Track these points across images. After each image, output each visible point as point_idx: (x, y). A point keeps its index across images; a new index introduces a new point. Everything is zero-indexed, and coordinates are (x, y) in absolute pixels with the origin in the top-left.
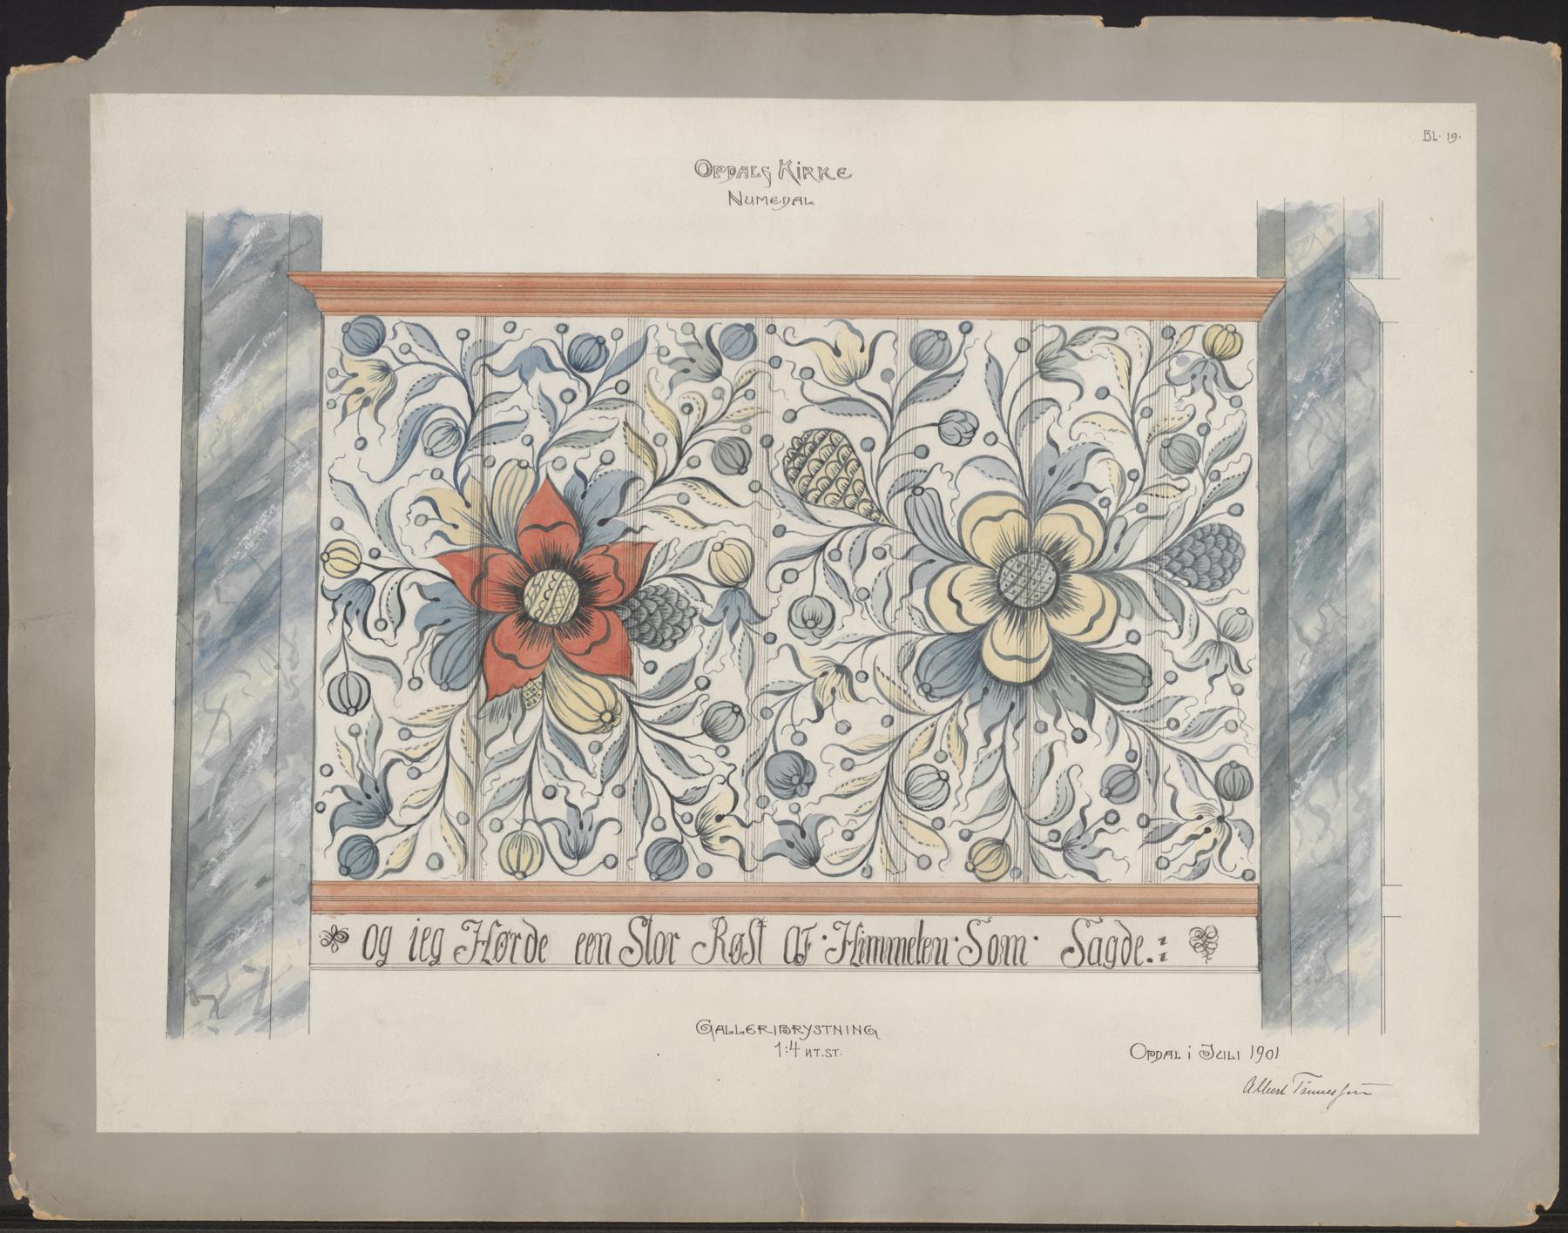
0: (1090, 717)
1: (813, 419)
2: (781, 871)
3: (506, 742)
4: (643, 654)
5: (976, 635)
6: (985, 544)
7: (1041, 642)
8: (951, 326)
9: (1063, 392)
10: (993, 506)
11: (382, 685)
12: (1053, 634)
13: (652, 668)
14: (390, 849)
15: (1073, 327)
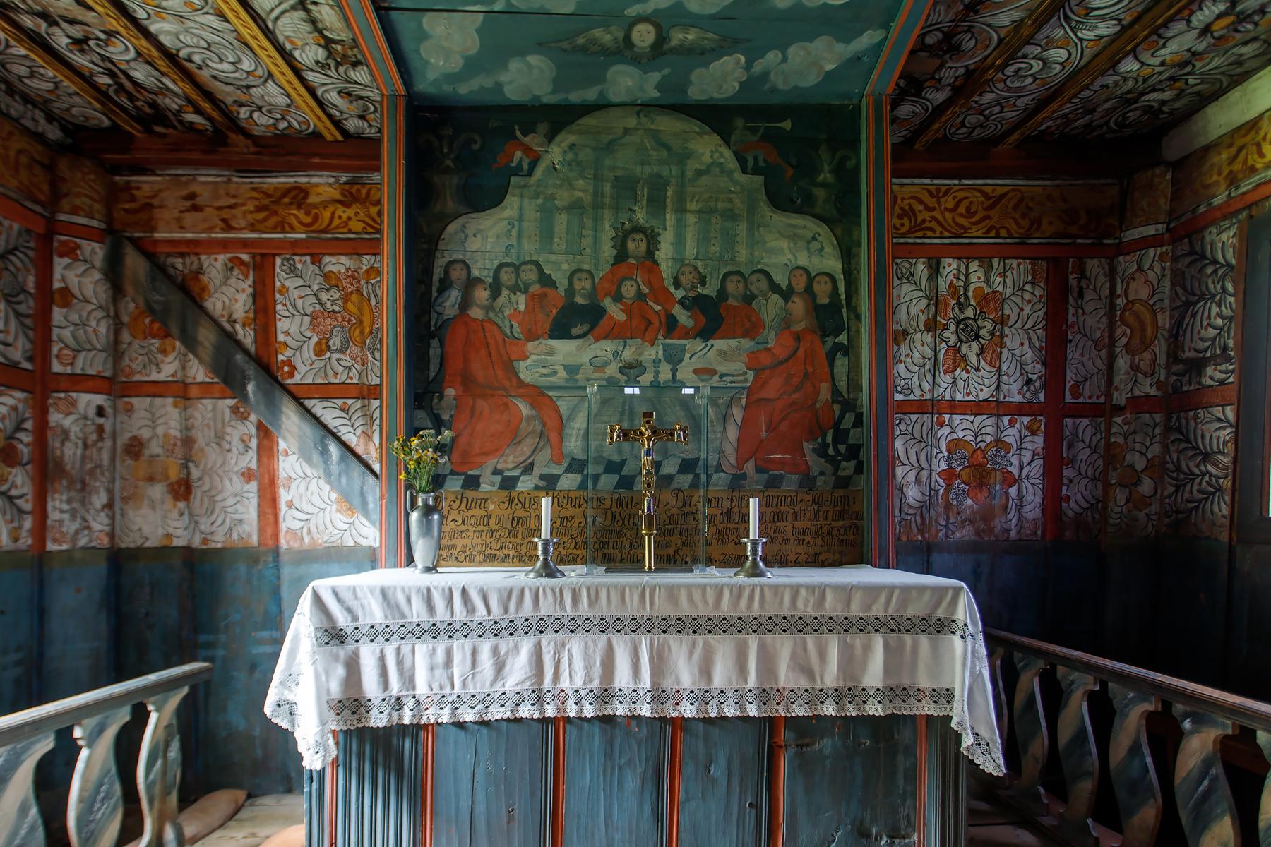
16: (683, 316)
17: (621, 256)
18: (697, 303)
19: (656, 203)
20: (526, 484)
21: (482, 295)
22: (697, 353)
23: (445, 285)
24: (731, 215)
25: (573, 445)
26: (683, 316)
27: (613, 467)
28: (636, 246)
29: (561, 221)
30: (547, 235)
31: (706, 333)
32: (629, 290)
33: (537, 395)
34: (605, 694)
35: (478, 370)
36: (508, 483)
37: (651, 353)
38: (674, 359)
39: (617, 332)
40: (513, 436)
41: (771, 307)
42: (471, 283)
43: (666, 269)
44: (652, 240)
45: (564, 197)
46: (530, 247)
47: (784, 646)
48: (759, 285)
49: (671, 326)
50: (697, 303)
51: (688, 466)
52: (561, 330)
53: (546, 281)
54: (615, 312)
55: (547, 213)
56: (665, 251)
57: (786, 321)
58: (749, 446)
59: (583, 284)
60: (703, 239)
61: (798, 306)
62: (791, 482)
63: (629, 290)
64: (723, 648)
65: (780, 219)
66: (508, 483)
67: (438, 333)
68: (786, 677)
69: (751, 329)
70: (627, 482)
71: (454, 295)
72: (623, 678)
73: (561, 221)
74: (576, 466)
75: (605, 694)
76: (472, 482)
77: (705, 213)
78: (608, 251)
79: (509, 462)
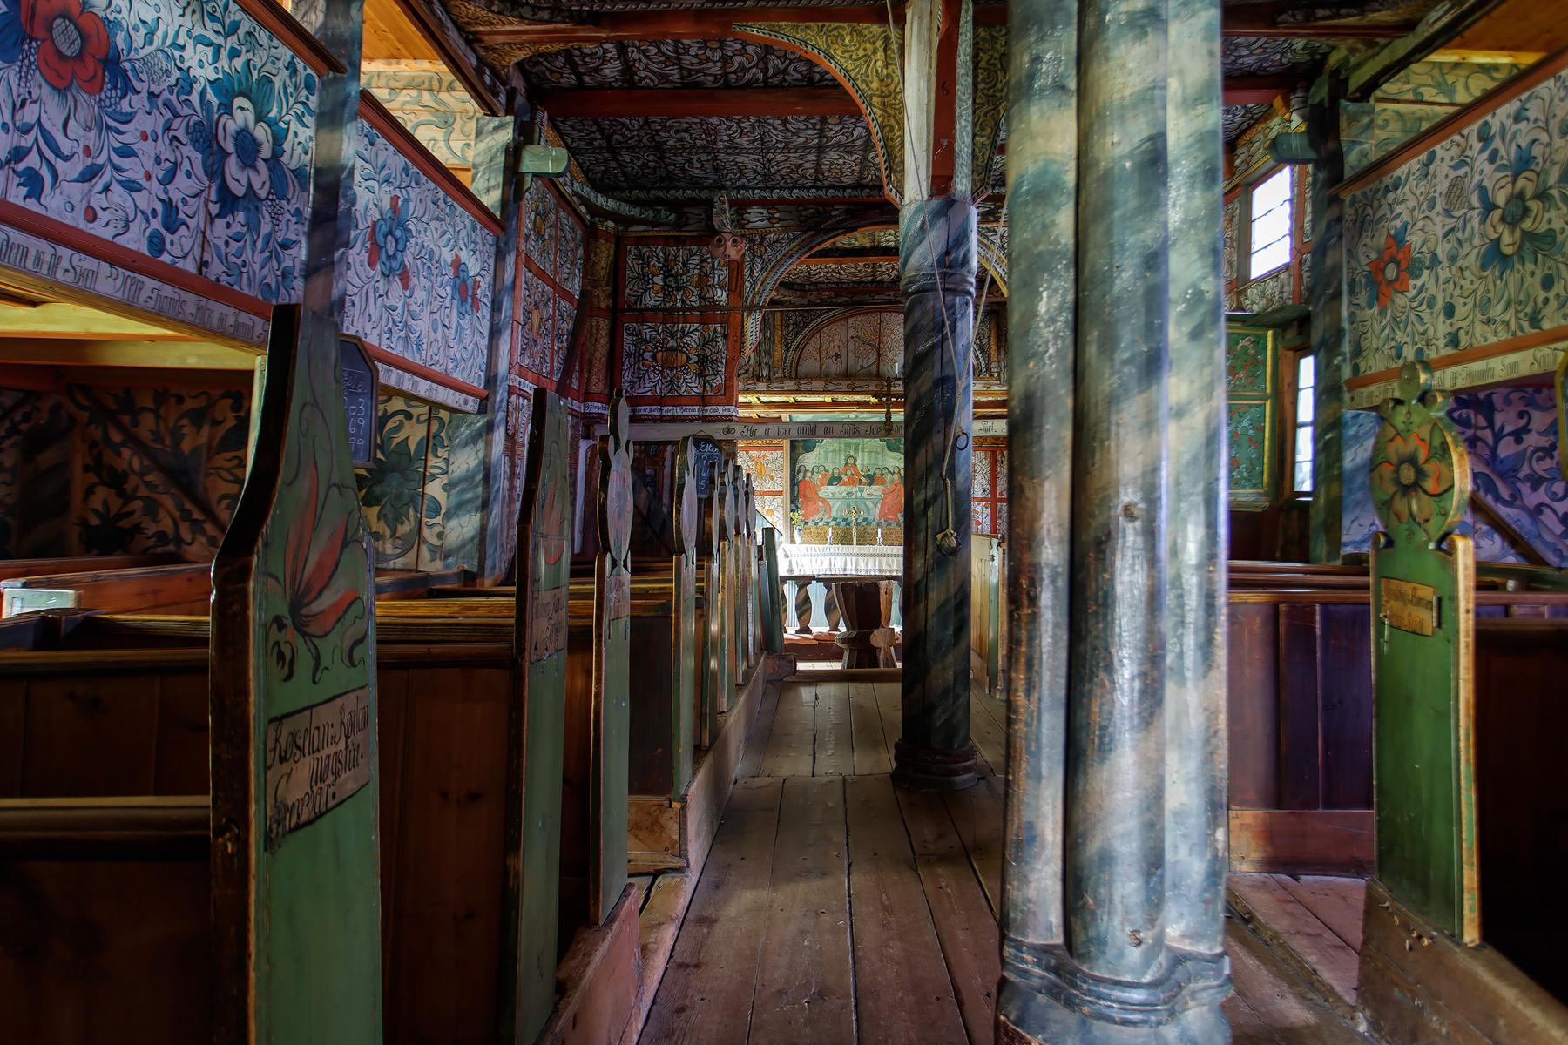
0: (1536, 262)
1: (1453, 174)
2: (1450, 351)
3: (1384, 322)
4: (1412, 282)
5: (1498, 240)
6: (1501, 199)
7: (1518, 233)
8: (1488, 118)
9: (1523, 125)
10: (1503, 182)
11: (1358, 312)
12: (1523, 231)
13: (1415, 287)
14: (1362, 366)
15: (1524, 97)
16: (864, 480)
17: (847, 464)
18: (868, 476)
19: (856, 450)
20: (821, 524)
21: (809, 474)
22: (868, 490)
23: (799, 471)
24: (877, 453)
25: (834, 514)
26: (864, 480)
27: (844, 520)
28: (851, 461)
29: (830, 455)
30: (826, 459)
31: (870, 484)
32: (849, 473)
33: (824, 500)
34: (845, 569)
35: (808, 494)
36: (816, 524)
37: (855, 489)
38: (861, 491)
39: (845, 484)
40: (818, 510)
41: (888, 477)
42: (806, 471)
43: (859, 467)
44: (855, 459)
45: (831, 448)
46: (822, 462)
47: (884, 560)
48: (885, 471)
49: (861, 482)
50: (868, 476)
51: (865, 519)
52: (830, 483)
53: (826, 471)
54: (845, 478)
55: (826, 453)
56: (858, 463)
57: (893, 481)
58: (882, 515)
59: (836, 471)
60: (869, 459)
61: (896, 477)
62: (894, 524)
63: (849, 473)
64: (871, 560)
65: (891, 453)
66: (816, 524)
67: (797, 484)
68: (885, 567)
69: (883, 483)
70: (849, 524)
71: (801, 474)
72: (849, 566)
73: (830, 455)
74: (835, 519)
75: (845, 569)
76: (807, 523)
77: (870, 452)
78: (843, 462)
79: (816, 518)
